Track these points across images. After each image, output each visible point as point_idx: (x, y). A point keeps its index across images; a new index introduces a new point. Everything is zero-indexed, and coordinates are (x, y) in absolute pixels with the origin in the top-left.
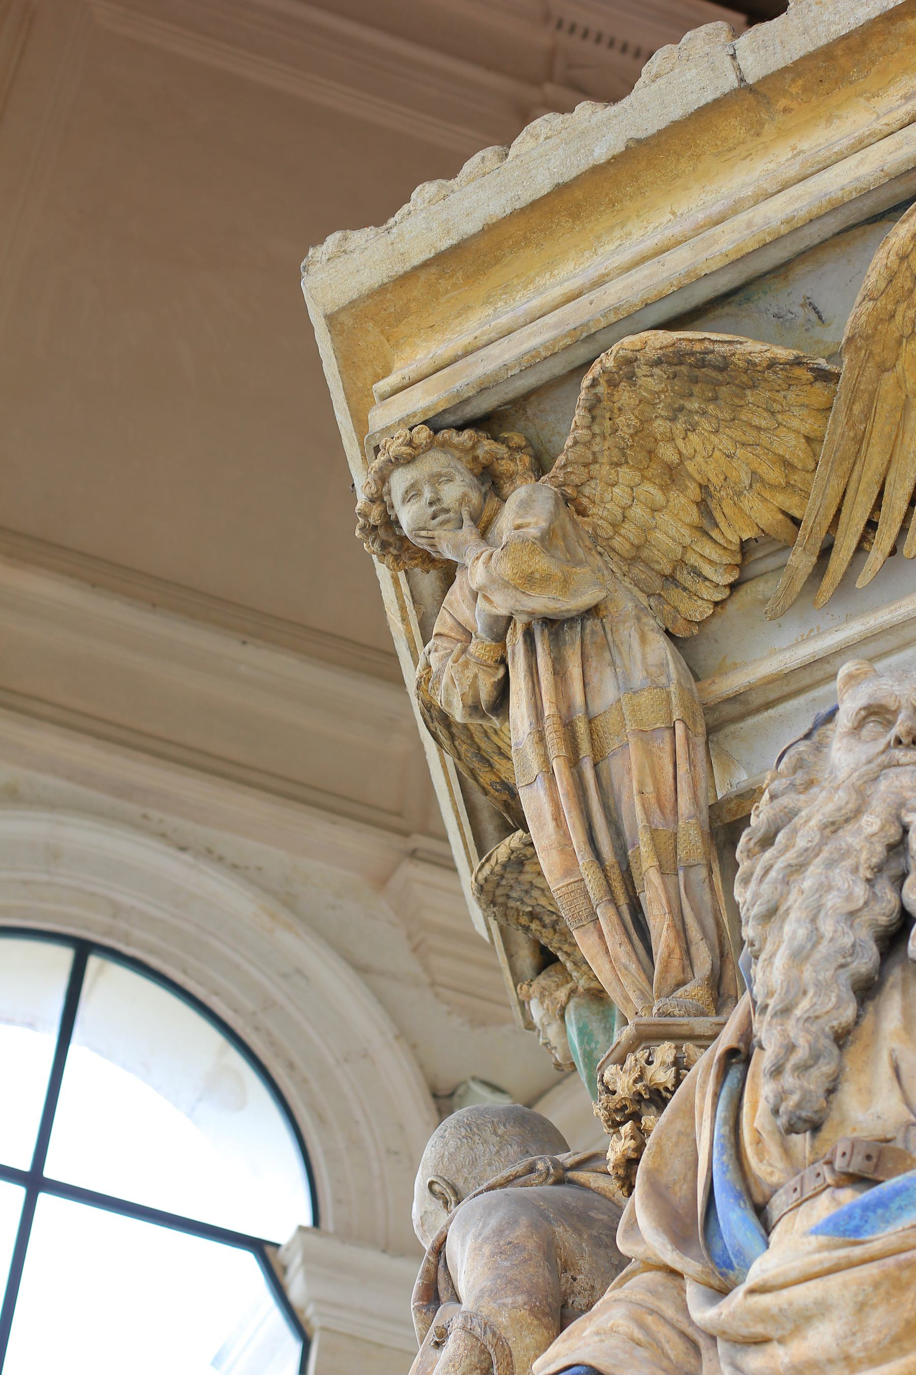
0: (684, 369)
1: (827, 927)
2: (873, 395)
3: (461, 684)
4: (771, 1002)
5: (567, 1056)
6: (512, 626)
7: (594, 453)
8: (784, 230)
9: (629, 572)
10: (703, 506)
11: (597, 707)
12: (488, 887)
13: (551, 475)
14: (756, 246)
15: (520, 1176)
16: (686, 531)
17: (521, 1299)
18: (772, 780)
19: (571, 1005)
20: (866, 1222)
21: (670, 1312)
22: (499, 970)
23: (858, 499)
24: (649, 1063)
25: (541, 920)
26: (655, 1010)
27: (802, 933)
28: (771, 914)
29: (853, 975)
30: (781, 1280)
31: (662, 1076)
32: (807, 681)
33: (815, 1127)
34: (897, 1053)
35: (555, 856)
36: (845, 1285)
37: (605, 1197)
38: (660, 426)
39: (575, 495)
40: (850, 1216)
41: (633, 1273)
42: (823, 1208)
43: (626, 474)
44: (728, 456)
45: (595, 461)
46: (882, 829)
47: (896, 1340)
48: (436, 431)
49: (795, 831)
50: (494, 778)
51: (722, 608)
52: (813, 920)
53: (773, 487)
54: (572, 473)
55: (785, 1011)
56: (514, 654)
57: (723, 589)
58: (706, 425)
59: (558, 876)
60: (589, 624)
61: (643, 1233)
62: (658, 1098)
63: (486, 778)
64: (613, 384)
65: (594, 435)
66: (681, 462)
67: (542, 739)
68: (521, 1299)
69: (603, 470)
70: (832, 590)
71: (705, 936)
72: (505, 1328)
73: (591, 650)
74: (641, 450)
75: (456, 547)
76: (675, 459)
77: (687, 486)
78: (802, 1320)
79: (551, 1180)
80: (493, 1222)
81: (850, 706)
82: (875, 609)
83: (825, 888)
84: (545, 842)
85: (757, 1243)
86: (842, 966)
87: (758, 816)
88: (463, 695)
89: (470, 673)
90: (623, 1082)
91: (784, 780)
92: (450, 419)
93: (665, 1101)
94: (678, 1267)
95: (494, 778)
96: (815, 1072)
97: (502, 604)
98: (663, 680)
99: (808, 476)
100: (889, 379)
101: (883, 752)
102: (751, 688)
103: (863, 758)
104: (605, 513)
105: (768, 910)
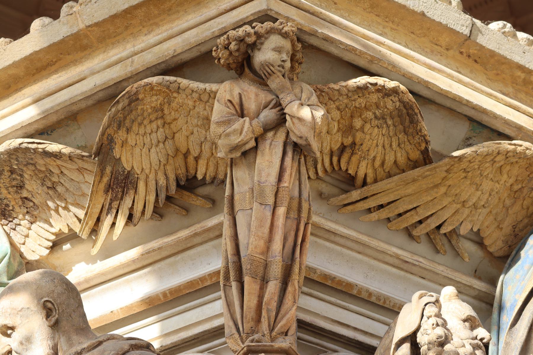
0: (405, 111)
8: (464, 102)
10: (343, 149)
14: (452, 97)
16: (328, 148)
43: (336, 114)
45: (334, 101)
54: (323, 96)
56: (271, 144)
59: (258, 251)
64: (378, 91)
66: (357, 131)
77: (347, 138)
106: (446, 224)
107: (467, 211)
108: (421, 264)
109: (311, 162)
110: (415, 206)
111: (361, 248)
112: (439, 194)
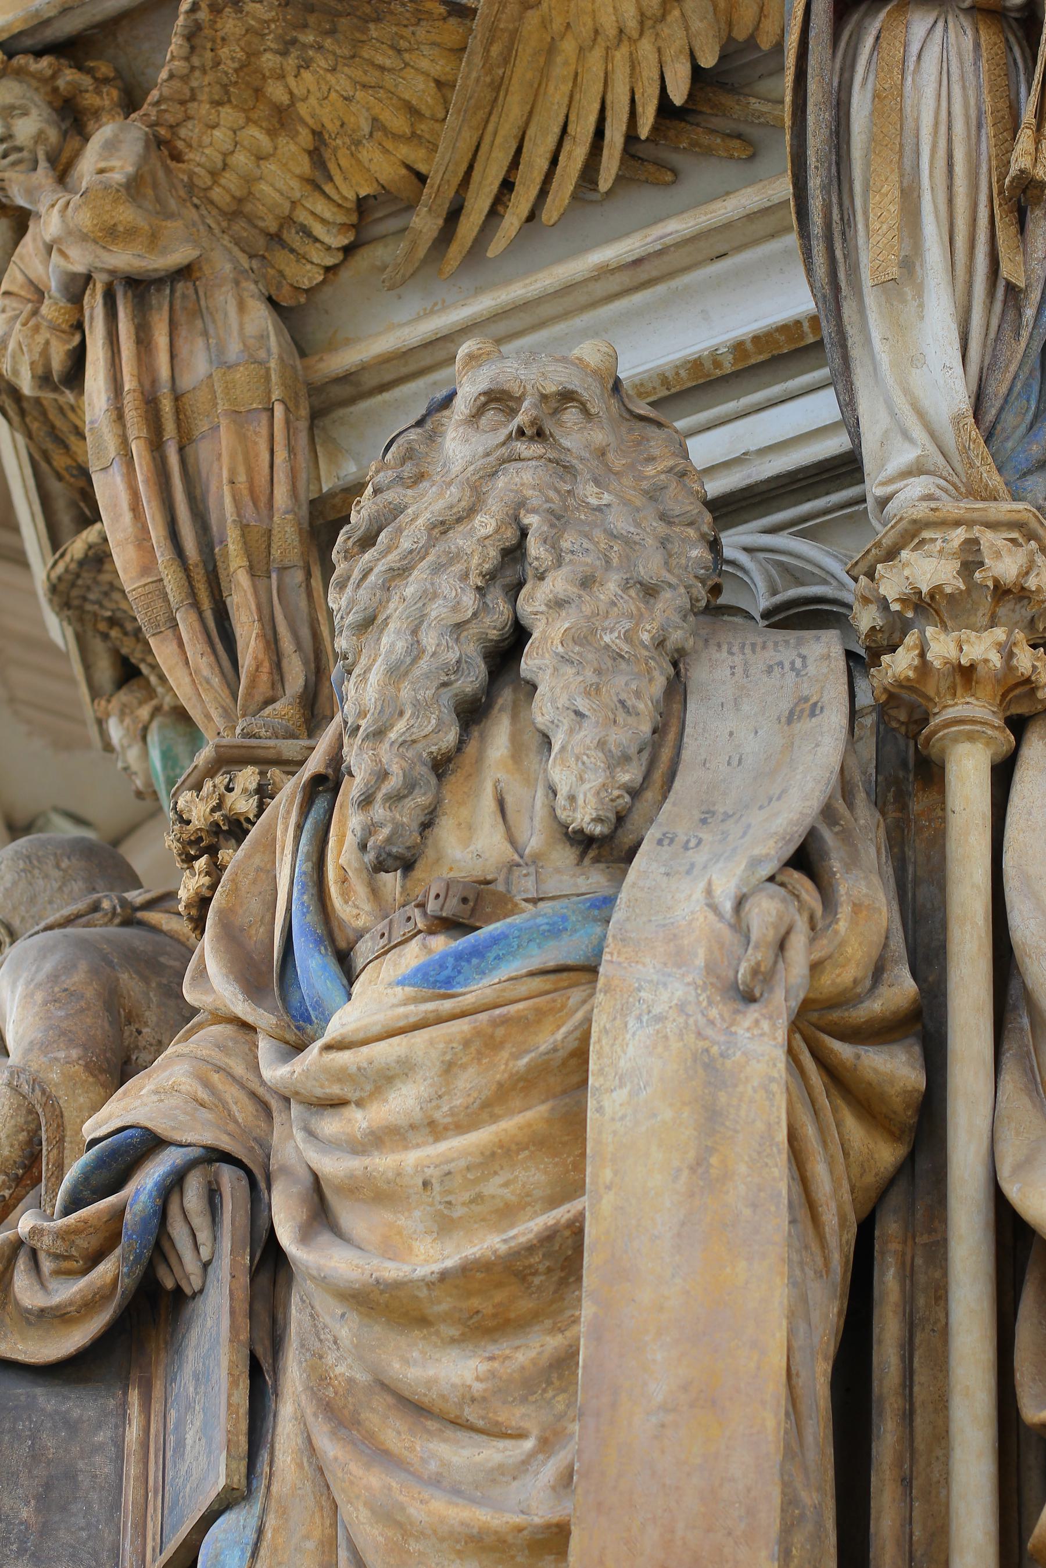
1: (429, 639)
2: (514, 35)
3: (30, 351)
4: (363, 723)
5: (149, 784)
6: (91, 286)
7: (192, 90)
9: (229, 228)
10: (317, 155)
11: (186, 382)
12: (62, 587)
13: (141, 112)
15: (82, 916)
16: (295, 184)
17: (75, 1053)
18: (377, 472)
19: (154, 726)
20: (459, 972)
21: (239, 1069)
22: (72, 681)
23: (493, 155)
24: (230, 790)
25: (122, 626)
26: (238, 731)
27: (401, 645)
28: (368, 623)
29: (456, 695)
30: (361, 1036)
31: (242, 804)
32: (427, 360)
33: (407, 865)
34: (502, 784)
35: (131, 552)
36: (432, 1043)
37: (178, 941)
38: (269, 61)
39: (168, 136)
40: (442, 965)
41: (200, 1026)
42: (412, 956)
43: (228, 115)
44: (346, 99)
45: (193, 98)
46: (497, 531)
47: (486, 1105)
48: (11, 56)
49: (400, 530)
50: (69, 462)
51: (335, 274)
52: (415, 632)
53: (397, 137)
55: (379, 734)
56: (92, 318)
57: (335, 252)
58: (321, 62)
59: (134, 574)
60: (180, 286)
61: (213, 981)
62: (236, 829)
63: (60, 461)
65: (193, 68)
66: (292, 104)
67: (120, 416)
68: (75, 1053)
69: (202, 109)
70: (459, 258)
71: (299, 648)
72: (56, 1085)
73: (181, 317)
74: (246, 89)
75: (30, 192)
76: (285, 99)
77: (298, 132)
78: (384, 1079)
79: (117, 921)
80: (48, 966)
81: (469, 389)
82: (507, 282)
83: (429, 595)
84: (120, 536)
85: (338, 994)
86: (445, 685)
87: (359, 512)
88: (32, 363)
89: (40, 339)
90: (199, 811)
91: (390, 472)
92: (28, 42)
93: (247, 832)
94: (250, 1019)
95: (69, 462)
96: (409, 803)
97: (79, 260)
98: (262, 354)
99: (437, 126)
100: (533, 18)
101: (504, 444)
102: (363, 368)
103: (481, 450)
104: (203, 159)
105: (364, 619)
106: (639, 109)
107: (646, 48)
108: (668, 241)
109: (298, 238)
110: (557, 130)
111: (525, 319)
112: (573, 60)
